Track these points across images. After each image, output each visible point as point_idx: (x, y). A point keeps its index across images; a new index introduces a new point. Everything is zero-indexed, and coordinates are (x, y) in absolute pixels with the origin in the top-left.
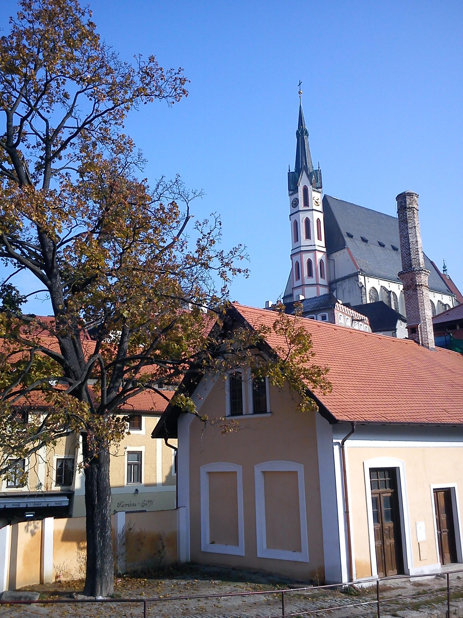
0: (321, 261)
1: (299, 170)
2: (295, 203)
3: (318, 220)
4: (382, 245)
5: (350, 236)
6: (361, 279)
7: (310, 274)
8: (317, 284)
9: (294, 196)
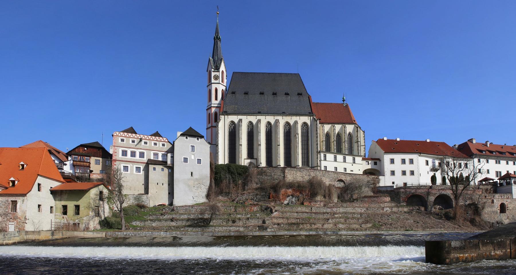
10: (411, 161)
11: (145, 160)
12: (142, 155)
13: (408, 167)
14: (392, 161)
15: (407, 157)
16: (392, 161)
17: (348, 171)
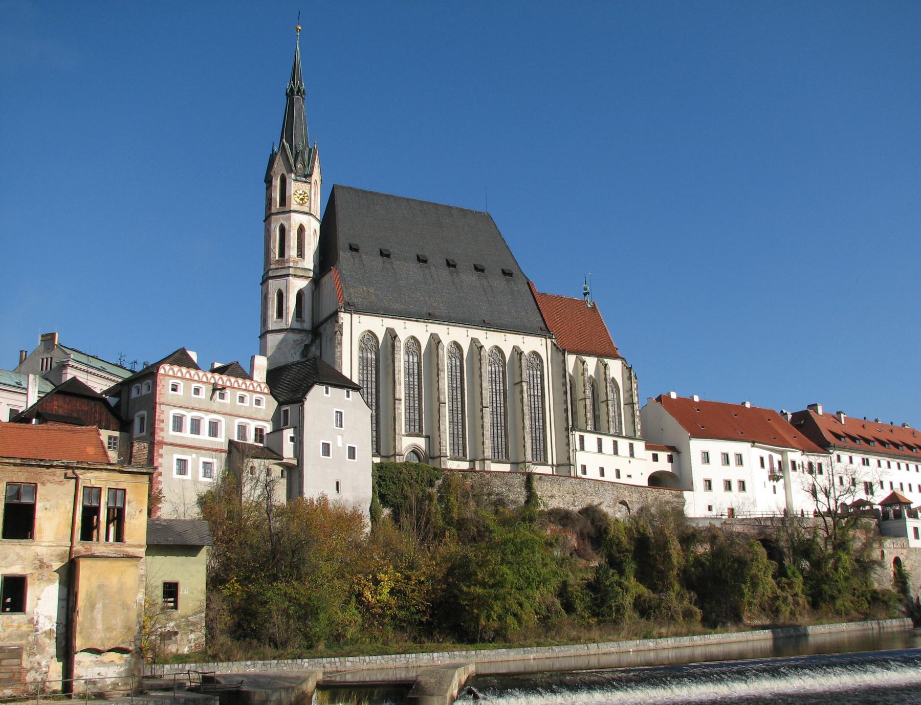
3: (301, 229)
4: (421, 260)
6: (344, 318)
10: (740, 460)
11: (221, 441)
12: (214, 430)
13: (734, 473)
14: (706, 458)
15: (733, 447)
16: (706, 458)
17: (624, 480)
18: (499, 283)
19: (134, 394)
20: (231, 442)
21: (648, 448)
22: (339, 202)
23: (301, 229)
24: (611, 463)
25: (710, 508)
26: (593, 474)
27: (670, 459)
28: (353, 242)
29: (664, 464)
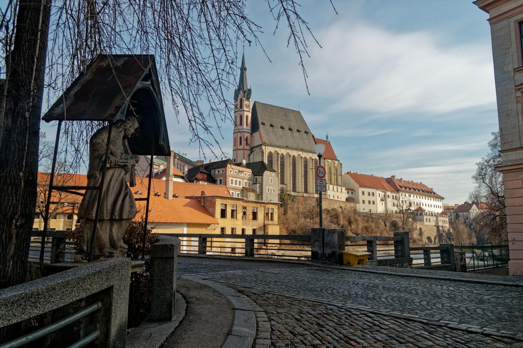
0: (247, 138)
1: (239, 89)
2: (236, 107)
4: (282, 128)
5: (263, 124)
6: (263, 147)
7: (241, 144)
8: (244, 149)
9: (236, 103)
13: (371, 198)
15: (371, 191)
17: (339, 199)
18: (305, 135)
19: (217, 172)
20: (243, 187)
21: (346, 189)
22: (257, 107)
23: (247, 117)
24: (336, 194)
25: (364, 209)
26: (331, 198)
27: (352, 193)
28: (263, 121)
29: (350, 195)
